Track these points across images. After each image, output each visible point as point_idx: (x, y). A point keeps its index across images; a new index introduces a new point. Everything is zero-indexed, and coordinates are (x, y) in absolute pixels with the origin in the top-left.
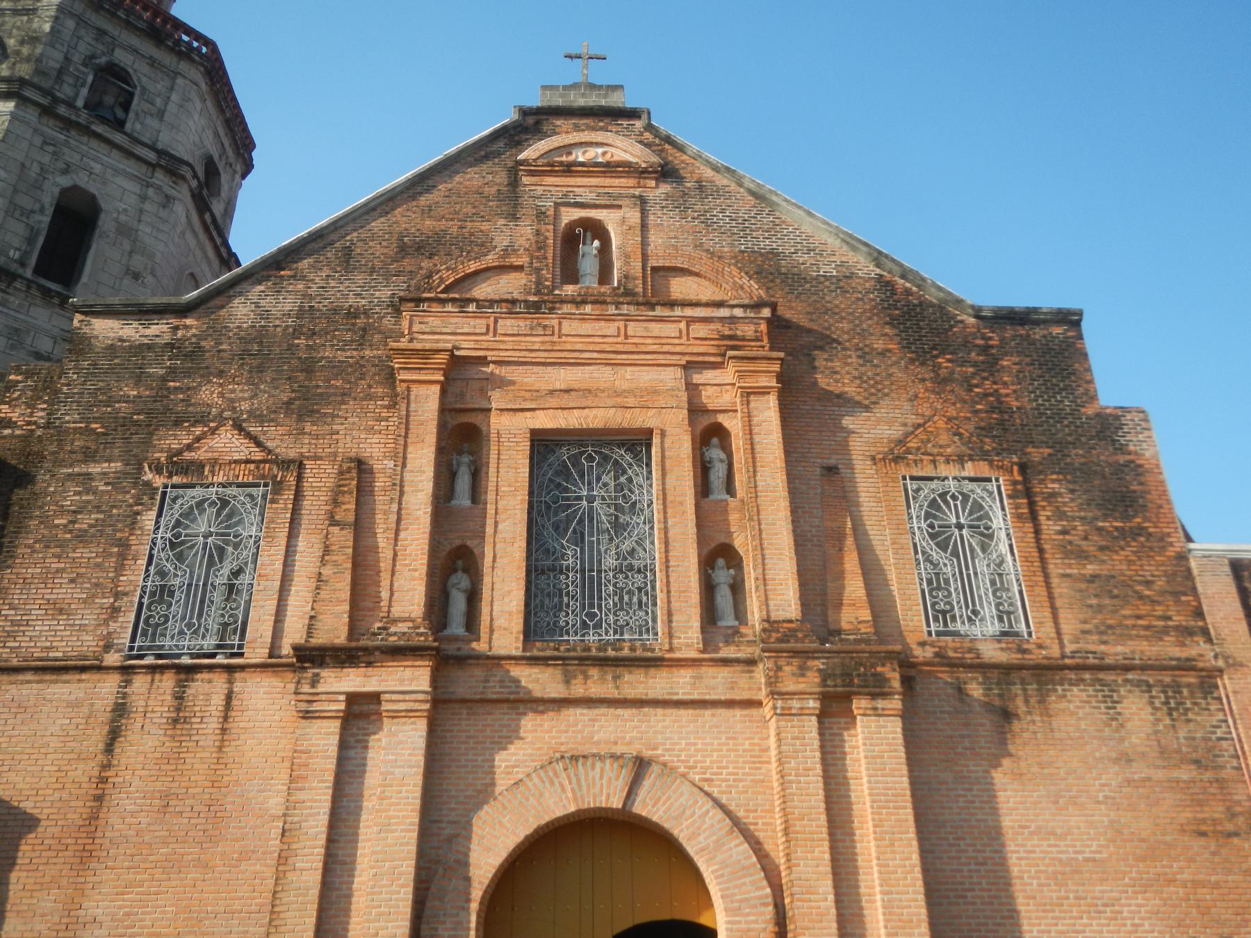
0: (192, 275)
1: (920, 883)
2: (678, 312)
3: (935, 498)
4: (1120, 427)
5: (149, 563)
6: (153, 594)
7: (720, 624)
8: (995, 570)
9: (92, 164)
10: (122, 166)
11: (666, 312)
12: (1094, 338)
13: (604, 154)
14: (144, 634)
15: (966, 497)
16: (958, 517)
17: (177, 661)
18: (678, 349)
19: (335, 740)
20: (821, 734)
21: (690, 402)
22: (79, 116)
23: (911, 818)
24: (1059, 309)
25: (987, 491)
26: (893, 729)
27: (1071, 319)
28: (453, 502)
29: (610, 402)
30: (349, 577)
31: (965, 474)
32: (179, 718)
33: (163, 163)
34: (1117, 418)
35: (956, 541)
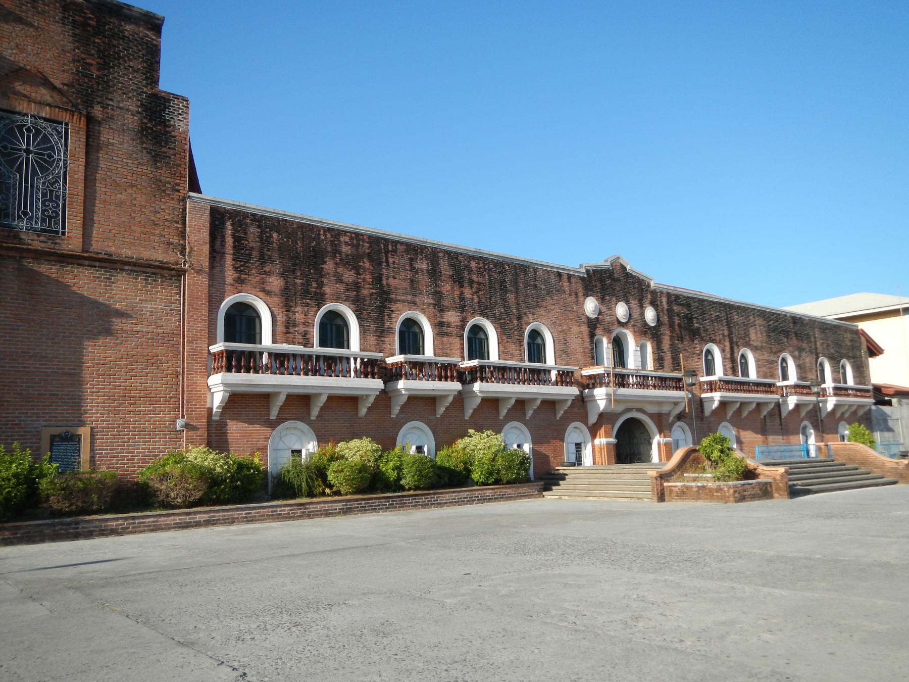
3: (13, 127)
4: (165, 108)
8: (48, 187)
15: (38, 132)
16: (28, 144)
24: (148, 12)
25: (57, 131)
27: (154, 24)
35: (22, 163)
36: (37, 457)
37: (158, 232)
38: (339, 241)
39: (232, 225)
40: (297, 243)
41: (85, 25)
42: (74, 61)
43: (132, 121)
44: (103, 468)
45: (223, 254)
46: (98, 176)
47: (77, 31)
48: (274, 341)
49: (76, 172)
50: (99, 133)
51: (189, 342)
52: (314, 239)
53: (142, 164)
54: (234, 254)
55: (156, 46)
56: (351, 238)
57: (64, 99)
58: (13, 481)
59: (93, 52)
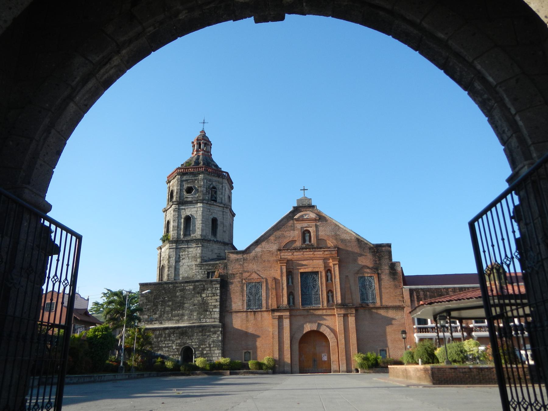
0: (231, 224)
1: (356, 339)
2: (322, 250)
5: (247, 296)
6: (248, 300)
7: (330, 302)
9: (215, 211)
10: (219, 209)
11: (320, 250)
12: (393, 249)
13: (309, 216)
14: (248, 306)
15: (368, 280)
17: (253, 310)
18: (322, 257)
19: (277, 322)
20: (343, 319)
21: (324, 266)
22: (211, 202)
23: (355, 331)
26: (354, 318)
27: (389, 246)
28: (289, 284)
29: (312, 267)
30: (276, 297)
31: (369, 276)
32: (255, 319)
33: (225, 206)
34: (395, 264)
36: (377, 355)
37: (397, 298)
38: (448, 291)
39: (416, 292)
40: (435, 294)
41: (374, 251)
42: (373, 261)
43: (387, 271)
44: (391, 358)
45: (414, 301)
46: (382, 287)
47: (373, 254)
48: (432, 323)
49: (377, 288)
50: (381, 276)
51: (408, 325)
52: (440, 292)
53: (391, 282)
54: (417, 300)
55: (390, 251)
56: (452, 289)
57: (372, 271)
58: (373, 360)
59: (377, 257)
